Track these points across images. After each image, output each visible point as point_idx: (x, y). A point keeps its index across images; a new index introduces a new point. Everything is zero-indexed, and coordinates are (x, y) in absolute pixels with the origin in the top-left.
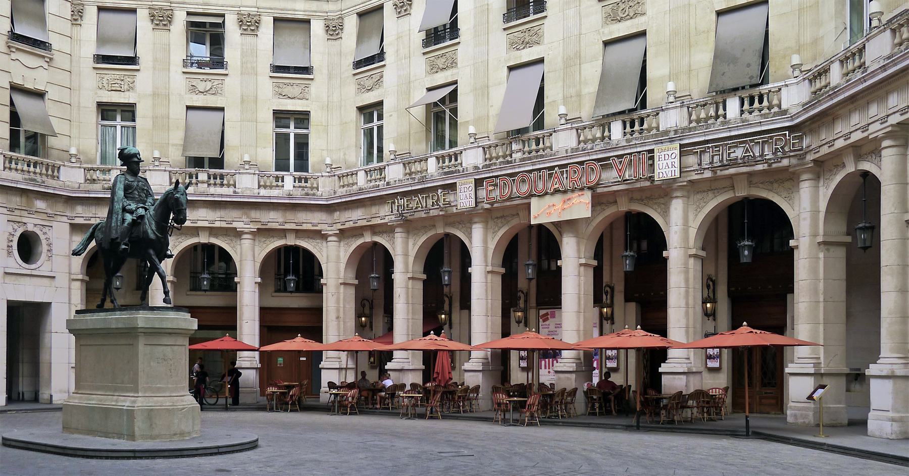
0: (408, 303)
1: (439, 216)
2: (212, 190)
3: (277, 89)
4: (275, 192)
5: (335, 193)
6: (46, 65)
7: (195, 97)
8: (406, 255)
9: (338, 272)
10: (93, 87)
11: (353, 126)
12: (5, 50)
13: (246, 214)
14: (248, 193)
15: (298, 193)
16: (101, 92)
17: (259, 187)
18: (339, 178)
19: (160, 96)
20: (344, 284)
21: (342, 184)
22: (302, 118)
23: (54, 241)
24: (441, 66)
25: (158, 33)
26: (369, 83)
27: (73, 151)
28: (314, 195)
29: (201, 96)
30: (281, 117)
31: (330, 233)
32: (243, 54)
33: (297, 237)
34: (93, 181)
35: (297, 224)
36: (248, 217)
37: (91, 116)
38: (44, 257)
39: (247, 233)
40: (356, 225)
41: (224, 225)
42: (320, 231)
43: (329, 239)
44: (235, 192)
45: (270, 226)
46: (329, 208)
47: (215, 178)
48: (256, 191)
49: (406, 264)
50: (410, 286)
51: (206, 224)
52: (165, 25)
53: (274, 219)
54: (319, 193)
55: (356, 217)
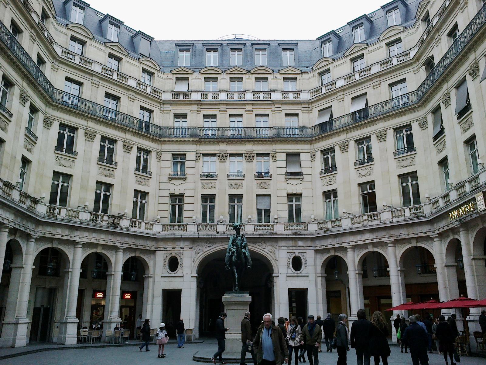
0: (473, 275)
1: (476, 218)
2: (370, 223)
4: (400, 219)
5: (432, 213)
6: (301, 182)
7: (361, 179)
8: (468, 244)
9: (442, 259)
10: (321, 186)
11: (438, 173)
13: (387, 233)
14: (387, 221)
17: (393, 217)
18: (433, 204)
20: (446, 266)
21: (434, 207)
22: (414, 175)
24: (467, 128)
26: (440, 147)
27: (313, 216)
28: (421, 216)
30: (403, 177)
31: (434, 236)
33: (417, 241)
34: (321, 229)
35: (415, 234)
36: (389, 235)
37: (320, 199)
38: (303, 267)
40: (444, 229)
41: (378, 240)
42: (429, 236)
43: (435, 240)
44: (381, 222)
46: (431, 222)
47: (371, 217)
48: (391, 220)
49: (469, 251)
50: (474, 264)
52: (345, 150)
53: (403, 233)
55: (442, 225)
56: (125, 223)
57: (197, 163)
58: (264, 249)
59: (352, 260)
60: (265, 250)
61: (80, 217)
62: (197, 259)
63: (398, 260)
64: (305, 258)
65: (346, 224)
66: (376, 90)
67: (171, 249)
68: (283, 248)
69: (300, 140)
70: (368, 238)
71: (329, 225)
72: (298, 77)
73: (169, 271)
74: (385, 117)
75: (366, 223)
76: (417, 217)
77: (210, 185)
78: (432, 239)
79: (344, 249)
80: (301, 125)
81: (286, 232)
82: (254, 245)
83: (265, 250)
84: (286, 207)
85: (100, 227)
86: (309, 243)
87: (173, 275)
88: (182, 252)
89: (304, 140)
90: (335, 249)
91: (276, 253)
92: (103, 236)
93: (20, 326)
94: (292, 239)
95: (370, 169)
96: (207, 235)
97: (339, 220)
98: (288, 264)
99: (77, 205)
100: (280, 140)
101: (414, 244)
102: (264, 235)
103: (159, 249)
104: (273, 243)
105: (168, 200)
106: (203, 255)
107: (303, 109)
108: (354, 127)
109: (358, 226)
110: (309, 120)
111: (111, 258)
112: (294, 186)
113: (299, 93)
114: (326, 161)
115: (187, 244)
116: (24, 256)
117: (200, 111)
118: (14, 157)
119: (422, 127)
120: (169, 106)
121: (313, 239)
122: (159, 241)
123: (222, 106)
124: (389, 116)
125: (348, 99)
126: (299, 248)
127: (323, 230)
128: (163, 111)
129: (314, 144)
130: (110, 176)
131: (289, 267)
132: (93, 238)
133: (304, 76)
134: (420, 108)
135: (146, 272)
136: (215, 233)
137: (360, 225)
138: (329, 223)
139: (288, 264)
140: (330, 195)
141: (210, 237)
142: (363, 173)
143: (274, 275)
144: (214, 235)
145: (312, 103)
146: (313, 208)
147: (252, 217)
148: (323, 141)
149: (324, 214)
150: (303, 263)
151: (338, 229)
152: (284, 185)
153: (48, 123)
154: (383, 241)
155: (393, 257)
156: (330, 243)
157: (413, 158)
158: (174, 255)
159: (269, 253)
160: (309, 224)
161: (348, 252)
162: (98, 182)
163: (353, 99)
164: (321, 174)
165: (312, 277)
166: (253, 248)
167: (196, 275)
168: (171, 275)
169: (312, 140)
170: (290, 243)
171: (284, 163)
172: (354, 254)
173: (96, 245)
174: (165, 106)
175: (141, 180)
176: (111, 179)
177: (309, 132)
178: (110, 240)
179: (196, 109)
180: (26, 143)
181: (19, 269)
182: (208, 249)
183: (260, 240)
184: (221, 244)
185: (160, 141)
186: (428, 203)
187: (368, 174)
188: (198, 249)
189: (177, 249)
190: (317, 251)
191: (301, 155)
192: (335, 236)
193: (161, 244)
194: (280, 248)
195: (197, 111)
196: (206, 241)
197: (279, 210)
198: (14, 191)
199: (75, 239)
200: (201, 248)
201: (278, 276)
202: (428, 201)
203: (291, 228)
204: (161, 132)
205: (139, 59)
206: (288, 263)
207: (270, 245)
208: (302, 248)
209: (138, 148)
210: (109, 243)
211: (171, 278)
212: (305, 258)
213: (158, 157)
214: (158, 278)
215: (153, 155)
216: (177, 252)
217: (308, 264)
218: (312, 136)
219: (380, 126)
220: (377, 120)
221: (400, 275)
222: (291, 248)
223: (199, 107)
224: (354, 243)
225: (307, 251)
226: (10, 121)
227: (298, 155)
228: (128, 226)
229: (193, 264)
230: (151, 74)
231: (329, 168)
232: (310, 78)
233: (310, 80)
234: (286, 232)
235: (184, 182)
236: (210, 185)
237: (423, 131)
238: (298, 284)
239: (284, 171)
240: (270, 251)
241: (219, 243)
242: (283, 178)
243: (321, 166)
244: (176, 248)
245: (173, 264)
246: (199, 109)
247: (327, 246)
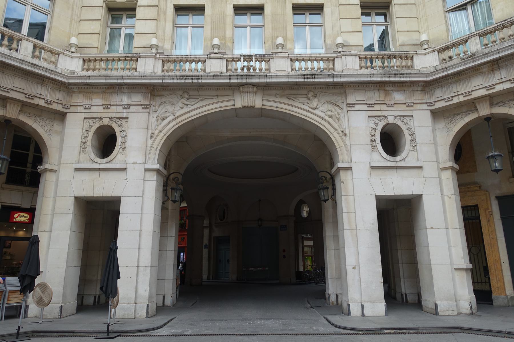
58: (315, 109)
60: (316, 112)
62: (161, 131)
64: (409, 129)
67: (99, 110)
68: (357, 107)
73: (93, 156)
82: (291, 102)
83: (316, 112)
86: (418, 96)
87: (102, 166)
88: (125, 115)
91: (342, 119)
94: (380, 86)
98: (372, 141)
103: (72, 109)
104: (332, 99)
105: (100, 13)
106: (174, 123)
115: (137, 98)
121: (428, 86)
122: (73, 92)
126: (396, 107)
131: (373, 147)
139: (372, 141)
141: (190, 81)
150: (407, 138)
158: (106, 122)
159: (327, 118)
160: (417, 54)
165: (430, 170)
166: (290, 108)
167: (157, 166)
168: (96, 166)
170: (375, 96)
182: (186, 110)
183: (304, 92)
184: (215, 100)
188: (164, 110)
189: (113, 108)
190: (437, 114)
193: (78, 99)
194: (352, 106)
196: (180, 93)
200: (169, 108)
201: (350, 169)
206: (373, 138)
207: (328, 102)
208: (404, 107)
211: (97, 173)
212: (409, 129)
214: (66, 173)
216: (114, 115)
217: (418, 141)
222: (377, 107)
225: (414, 113)
229: (150, 142)
238: (398, 185)
240: (329, 113)
244: (112, 107)
245: (106, 143)
247: (469, 93)
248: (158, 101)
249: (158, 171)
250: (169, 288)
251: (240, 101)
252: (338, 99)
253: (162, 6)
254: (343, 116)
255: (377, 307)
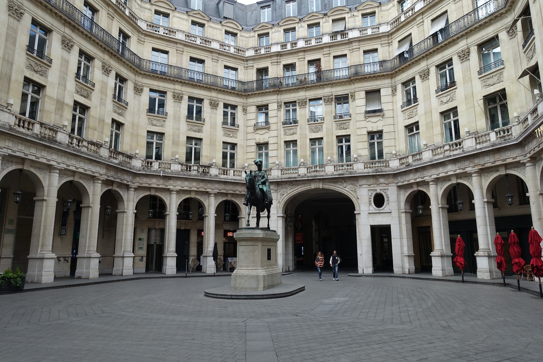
3: (484, 84)
4: (485, 145)
6: (381, 119)
9: (536, 186)
10: (403, 121)
12: (364, 119)
15: (499, 141)
16: (405, 121)
19: (429, 112)
23: (389, 195)
25: (424, 82)
28: (509, 139)
29: (446, 105)
31: (525, 161)
32: (464, 73)
34: (403, 164)
35: (503, 160)
37: (402, 133)
39: (474, 173)
40: (535, 152)
41: (461, 171)
42: (518, 162)
43: (527, 165)
44: (463, 151)
45: (487, 165)
51: (452, 173)
53: (488, 161)
54: (513, 137)
56: (214, 171)
57: (279, 112)
59: (435, 194)
60: (345, 189)
61: (172, 168)
63: (485, 191)
64: (387, 195)
65: (427, 156)
66: (457, 4)
68: (363, 186)
69: (379, 76)
70: (451, 170)
71: (410, 160)
72: (377, 10)
74: (467, 33)
75: (447, 153)
76: (505, 140)
77: (292, 131)
78: (524, 164)
79: (426, 183)
80: (381, 60)
81: (366, 170)
82: (335, 185)
83: (346, 189)
84: (366, 145)
85: (190, 176)
86: (391, 180)
89: (383, 75)
90: (418, 184)
92: (194, 184)
93: (126, 259)
94: (373, 176)
95: (452, 94)
96: (289, 178)
97: (420, 153)
99: (170, 158)
100: (358, 79)
101: (502, 172)
102: (343, 174)
104: (353, 182)
105: (254, 149)
107: (383, 42)
108: (434, 51)
109: (440, 158)
110: (389, 53)
111: (204, 202)
112: (375, 124)
113: (378, 26)
114: (408, 93)
116: (126, 203)
117: (280, 62)
118: (102, 121)
119: (512, 35)
120: (252, 62)
121: (395, 175)
123: (300, 54)
124: (471, 31)
125: (427, 22)
127: (404, 166)
128: (247, 67)
129: (395, 77)
130: (200, 131)
131: (370, 204)
132: (186, 185)
133: (383, 8)
134: (509, 12)
135: (240, 213)
136: (296, 175)
137: (441, 156)
138: (410, 157)
140: (412, 128)
142: (445, 100)
143: (355, 212)
144: (295, 178)
145: (392, 34)
146: (395, 144)
147: (332, 157)
148: (403, 72)
149: (406, 148)
150: (386, 199)
151: (419, 162)
152: (363, 124)
153: (138, 90)
154: (466, 172)
155: (478, 187)
156: (412, 178)
157: (501, 74)
159: (350, 191)
161: (430, 186)
162: (188, 138)
163: (433, 20)
164: (402, 107)
165: (395, 213)
167: (282, 215)
169: (392, 74)
170: (371, 181)
171: (363, 102)
172: (437, 187)
173: (189, 192)
174: (249, 63)
175: (229, 133)
176: (199, 134)
177: (389, 65)
178: (202, 187)
179: (276, 61)
180: (115, 109)
181: (122, 214)
182: (292, 190)
184: (303, 186)
185: (245, 96)
186: (517, 123)
187: (450, 100)
190: (400, 187)
191: (381, 90)
192: (417, 170)
194: (360, 186)
195: (277, 62)
197: (360, 148)
198: (102, 149)
199: (208, 190)
200: (285, 190)
201: (360, 214)
202: (517, 120)
203: (371, 166)
204: (246, 87)
205: (221, 22)
207: (351, 184)
208: (384, 185)
209: (224, 104)
210: (200, 190)
213: (245, 110)
215: (240, 109)
217: (390, 200)
218: (392, 69)
219: (462, 45)
220: (458, 38)
221: (486, 207)
222: (372, 186)
223: (279, 58)
224: (435, 176)
225: (389, 188)
226: (93, 90)
227: (378, 91)
228: (218, 174)
229: (278, 205)
230: (234, 35)
231: (411, 100)
232: (390, 9)
233: (390, 11)
234: (366, 170)
235: (268, 131)
236: (292, 131)
237: (512, 40)
239: (363, 109)
241: (301, 184)
242: (362, 117)
243: (403, 99)
246: (279, 61)
247: (409, 181)
248: (280, 187)
249: (282, 217)
250: (291, 264)
251: (313, 186)
252: (356, 183)
253: (279, 143)
254: (358, 191)
255: (369, 270)
